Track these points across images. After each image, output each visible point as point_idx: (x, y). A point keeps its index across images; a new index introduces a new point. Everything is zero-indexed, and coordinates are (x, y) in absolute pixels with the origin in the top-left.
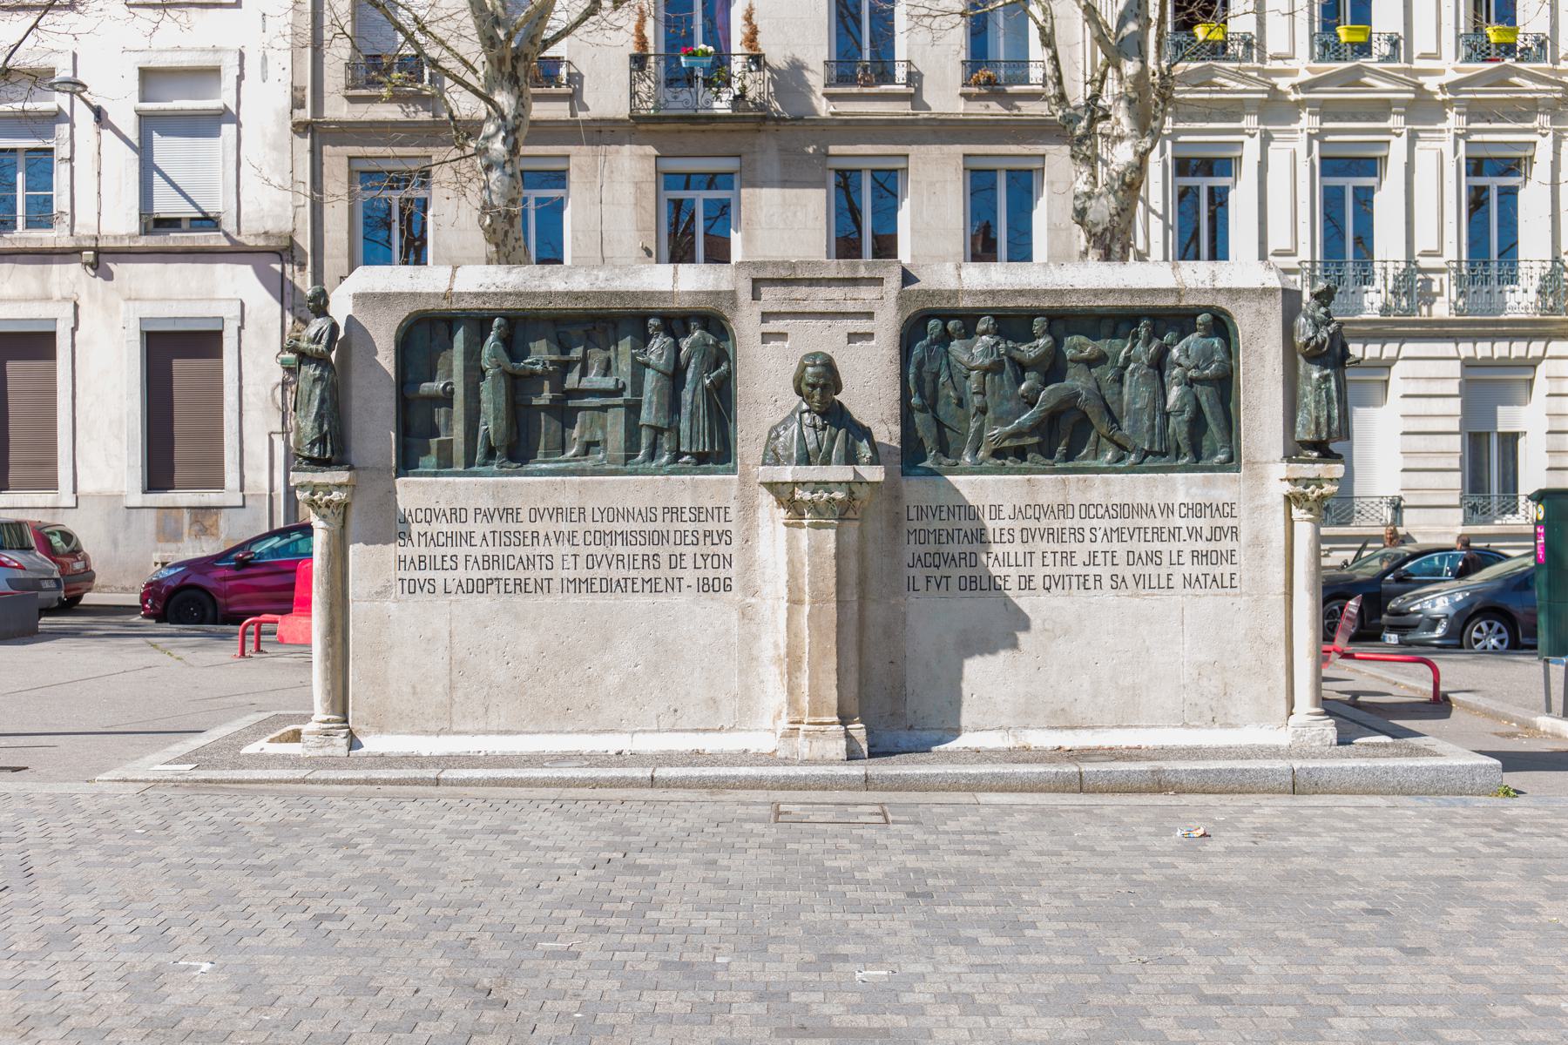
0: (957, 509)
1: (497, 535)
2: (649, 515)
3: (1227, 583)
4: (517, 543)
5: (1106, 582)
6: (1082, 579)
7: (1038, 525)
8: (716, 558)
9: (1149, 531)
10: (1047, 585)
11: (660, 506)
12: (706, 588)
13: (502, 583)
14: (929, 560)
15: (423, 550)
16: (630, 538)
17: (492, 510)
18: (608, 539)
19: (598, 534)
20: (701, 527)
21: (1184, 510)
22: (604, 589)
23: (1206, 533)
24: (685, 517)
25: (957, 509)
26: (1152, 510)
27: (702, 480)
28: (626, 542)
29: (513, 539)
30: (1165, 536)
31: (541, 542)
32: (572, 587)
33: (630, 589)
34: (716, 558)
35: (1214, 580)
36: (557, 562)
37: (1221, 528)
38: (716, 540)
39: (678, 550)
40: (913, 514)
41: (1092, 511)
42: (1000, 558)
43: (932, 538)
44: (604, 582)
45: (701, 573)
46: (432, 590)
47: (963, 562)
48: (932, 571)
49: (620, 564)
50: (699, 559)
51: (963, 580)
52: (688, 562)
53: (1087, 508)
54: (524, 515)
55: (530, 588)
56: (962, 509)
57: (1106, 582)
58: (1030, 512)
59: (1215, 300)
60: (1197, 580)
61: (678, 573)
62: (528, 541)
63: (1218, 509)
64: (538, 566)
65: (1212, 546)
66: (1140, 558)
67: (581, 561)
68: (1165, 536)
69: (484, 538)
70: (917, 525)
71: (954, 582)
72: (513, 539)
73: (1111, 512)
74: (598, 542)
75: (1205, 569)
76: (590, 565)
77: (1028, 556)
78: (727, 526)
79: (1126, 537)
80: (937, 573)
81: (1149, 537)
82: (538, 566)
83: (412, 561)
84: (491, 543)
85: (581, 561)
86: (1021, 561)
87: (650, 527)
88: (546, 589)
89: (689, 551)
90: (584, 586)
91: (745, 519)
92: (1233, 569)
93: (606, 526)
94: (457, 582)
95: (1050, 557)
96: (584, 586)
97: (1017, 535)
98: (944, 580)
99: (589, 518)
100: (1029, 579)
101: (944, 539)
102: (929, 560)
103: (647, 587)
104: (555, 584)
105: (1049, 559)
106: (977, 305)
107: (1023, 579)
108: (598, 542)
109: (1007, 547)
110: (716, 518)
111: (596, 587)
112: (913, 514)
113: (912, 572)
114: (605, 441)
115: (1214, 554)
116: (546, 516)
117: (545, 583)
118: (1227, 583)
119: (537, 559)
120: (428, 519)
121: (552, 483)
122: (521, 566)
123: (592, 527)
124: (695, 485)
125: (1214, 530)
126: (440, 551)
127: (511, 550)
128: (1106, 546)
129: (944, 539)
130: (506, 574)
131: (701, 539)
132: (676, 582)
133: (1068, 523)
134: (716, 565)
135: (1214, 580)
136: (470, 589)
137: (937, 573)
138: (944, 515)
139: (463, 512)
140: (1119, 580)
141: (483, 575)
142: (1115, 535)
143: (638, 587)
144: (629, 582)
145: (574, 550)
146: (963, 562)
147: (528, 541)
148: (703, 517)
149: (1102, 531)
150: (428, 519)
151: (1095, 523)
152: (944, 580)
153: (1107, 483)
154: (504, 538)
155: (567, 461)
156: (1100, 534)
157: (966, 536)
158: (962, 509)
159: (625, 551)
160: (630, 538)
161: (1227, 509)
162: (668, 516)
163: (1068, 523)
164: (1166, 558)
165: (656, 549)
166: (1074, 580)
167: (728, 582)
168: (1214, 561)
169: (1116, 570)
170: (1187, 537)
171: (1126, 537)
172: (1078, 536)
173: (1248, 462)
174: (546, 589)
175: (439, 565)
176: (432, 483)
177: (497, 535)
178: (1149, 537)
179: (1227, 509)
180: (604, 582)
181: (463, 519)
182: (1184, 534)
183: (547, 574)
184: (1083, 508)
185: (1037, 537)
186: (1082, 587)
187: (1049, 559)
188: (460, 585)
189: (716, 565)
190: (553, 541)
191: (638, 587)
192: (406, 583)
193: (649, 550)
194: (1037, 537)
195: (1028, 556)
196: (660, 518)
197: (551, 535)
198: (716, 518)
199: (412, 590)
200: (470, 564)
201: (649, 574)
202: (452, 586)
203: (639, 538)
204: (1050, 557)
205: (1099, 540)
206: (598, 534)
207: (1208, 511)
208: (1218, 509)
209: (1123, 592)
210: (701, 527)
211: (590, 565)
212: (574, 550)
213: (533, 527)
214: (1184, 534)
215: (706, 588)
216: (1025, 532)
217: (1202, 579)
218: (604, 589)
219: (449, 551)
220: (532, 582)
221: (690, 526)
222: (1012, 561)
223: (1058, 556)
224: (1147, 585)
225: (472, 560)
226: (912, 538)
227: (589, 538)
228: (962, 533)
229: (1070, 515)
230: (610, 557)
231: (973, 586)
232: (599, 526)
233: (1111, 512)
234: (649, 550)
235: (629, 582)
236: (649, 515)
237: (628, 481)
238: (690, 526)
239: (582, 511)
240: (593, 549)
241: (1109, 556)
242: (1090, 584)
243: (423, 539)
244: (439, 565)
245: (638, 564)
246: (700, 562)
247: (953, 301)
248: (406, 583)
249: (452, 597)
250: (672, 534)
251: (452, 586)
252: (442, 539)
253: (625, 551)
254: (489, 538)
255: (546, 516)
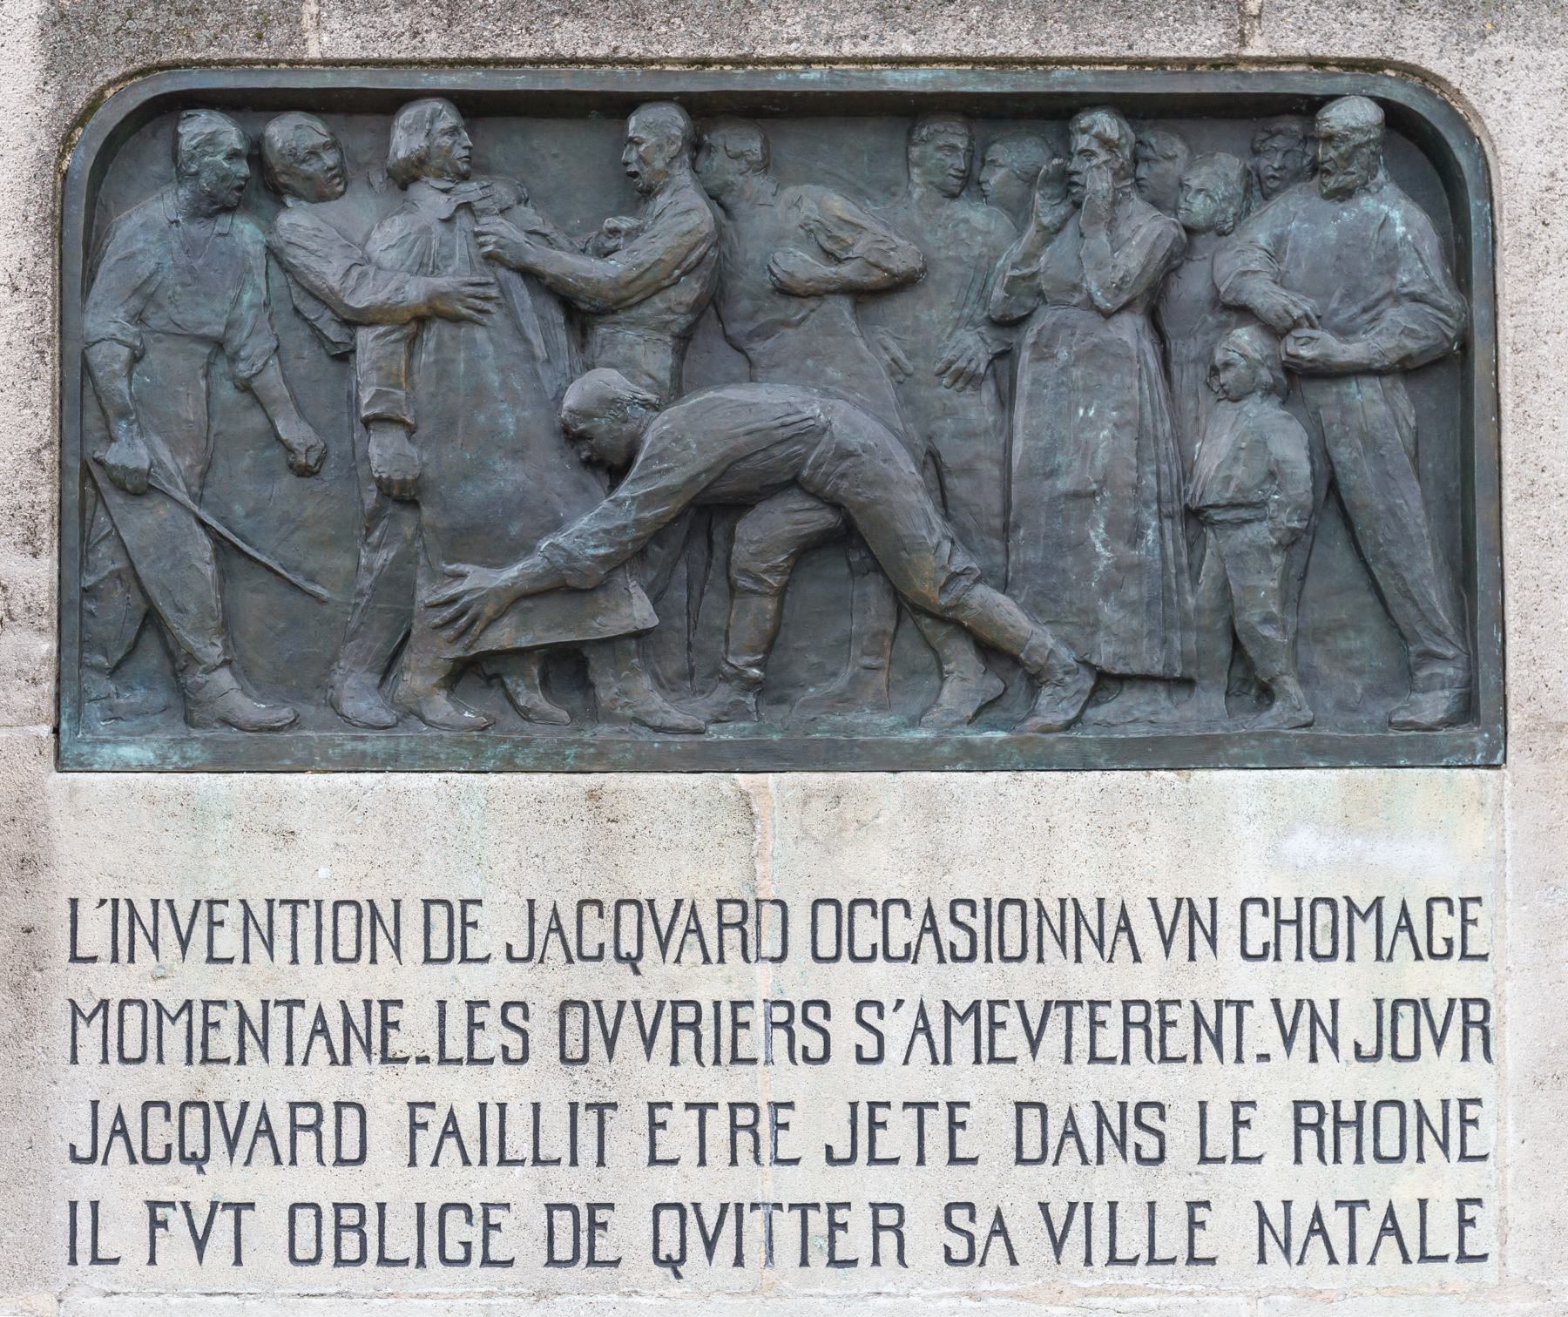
0: (282, 915)
3: (1443, 1239)
5: (926, 1234)
6: (818, 1221)
7: (631, 987)
9: (1112, 1016)
10: (670, 1247)
14: (162, 1132)
21: (1261, 929)
23: (1357, 1027)
25: (282, 915)
26: (1125, 926)
30: (1180, 1040)
35: (1390, 1226)
37: (1420, 1006)
40: (95, 935)
41: (867, 930)
42: (468, 1126)
43: (175, 1036)
47: (306, 1141)
48: (174, 1182)
51: (305, 1218)
53: (846, 914)
56: (307, 917)
57: (926, 1234)
58: (597, 932)
59: (1390, 36)
60: (1317, 1226)
63: (1405, 923)
65: (1382, 1080)
66: (1071, 1130)
68: (1180, 1040)
70: (114, 982)
71: (266, 1229)
73: (948, 932)
75: (1349, 1179)
77: (588, 1122)
79: (1011, 1041)
80: (198, 1189)
81: (1110, 1042)
86: (555, 1142)
92: (1469, 1180)
95: (682, 1124)
97: (542, 1029)
98: (225, 1219)
100: (593, 1218)
101: (224, 1042)
102: (162, 1132)
105: (679, 1135)
106: (382, 50)
107: (563, 1220)
109: (501, 1083)
112: (95, 935)
113: (88, 1182)
115: (1390, 1116)
118: (1443, 1239)
125: (1388, 1012)
128: (923, 1080)
129: (224, 1042)
133: (762, 982)
135: (1390, 1226)
137: (198, 1189)
138: (228, 943)
140: (981, 1229)
142: (963, 1035)
146: (306, 1141)
149: (909, 1015)
151: (879, 979)
152: (225, 1219)
153: (932, 812)
156: (898, 1028)
157: (320, 1028)
158: (307, 917)
161: (1447, 926)
163: (762, 982)
164: (1181, 1133)
166: (787, 1224)
168: (1390, 1147)
169: (961, 1183)
170: (1274, 1043)
171: (1011, 1041)
172: (805, 1036)
173: (1540, 723)
178: (1110, 1042)
179: (1447, 926)
182: (1262, 1031)
184: (827, 914)
185: (629, 1037)
186: (818, 1257)
187: (679, 1135)
194: (629, 1037)
195: (588, 1122)
204: (682, 1124)
205: (894, 1052)
207: (1365, 932)
208: (1405, 923)
209: (994, 1274)
214: (1262, 1031)
216: (575, 1019)
217: (1336, 1222)
222: (519, 1145)
223: (718, 1123)
224: (1100, 1252)
226: (89, 1036)
228: (304, 1020)
229: (771, 947)
231: (350, 1249)
233: (948, 932)
241: (937, 1122)
242: (856, 1241)
247: (279, 33)
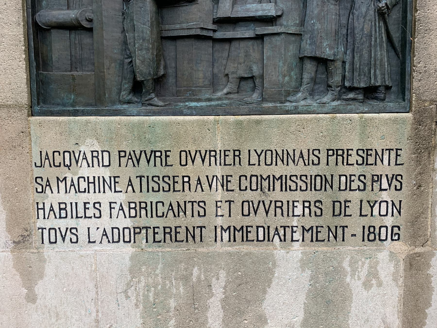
1: (144, 180)
2: (312, 157)
4: (167, 188)
8: (384, 205)
11: (323, 148)
12: (372, 237)
13: (151, 231)
15: (63, 197)
16: (289, 182)
17: (138, 153)
18: (265, 184)
19: (254, 179)
20: (369, 171)
22: (261, 238)
24: (352, 160)
27: (371, 119)
28: (285, 188)
29: (162, 184)
31: (193, 187)
32: (226, 236)
33: (288, 237)
34: (384, 205)
36: (211, 209)
38: (385, 185)
39: (342, 196)
44: (261, 230)
45: (366, 221)
46: (74, 240)
49: (279, 211)
50: (365, 205)
52: (353, 209)
54: (173, 159)
55: (181, 236)
61: (342, 221)
62: (179, 187)
64: (189, 212)
67: (236, 208)
69: (130, 183)
72: (162, 184)
74: (254, 187)
76: (246, 212)
78: (397, 170)
82: (189, 212)
83: (52, 209)
84: (137, 188)
85: (236, 208)
87: (313, 171)
88: (198, 238)
89: (355, 196)
90: (238, 235)
91: (418, 162)
93: (264, 171)
94: (101, 231)
96: (238, 235)
99: (245, 161)
103: (308, 235)
104: (208, 234)
108: (254, 187)
110: (386, 161)
111: (252, 236)
114: (262, 77)
116: (198, 159)
117: (197, 231)
119: (189, 206)
120: (67, 162)
121: (205, 123)
122: (171, 213)
123: (249, 171)
124: (364, 124)
126: (82, 198)
127: (160, 197)
130: (154, 222)
131: (369, 183)
132: (340, 231)
134: (383, 212)
136: (116, 239)
139: (106, 155)
141: (129, 223)
143: (297, 236)
144: (288, 231)
145: (229, 196)
147: (179, 187)
148: (371, 160)
150: (67, 162)
154: (152, 184)
155: (219, 99)
159: (284, 197)
160: (289, 182)
162: (332, 159)
165: (318, 196)
167: (396, 230)
174: (198, 238)
175: (81, 213)
176: (69, 122)
177: (144, 180)
180: (261, 230)
181: (106, 163)
183: (199, 222)
188: (105, 234)
189: (383, 212)
190: (206, 186)
191: (297, 236)
192: (46, 233)
193: (312, 196)
196: (323, 160)
197: (204, 180)
198: (386, 161)
199: (53, 240)
200: (115, 212)
201: (310, 222)
202: (96, 235)
203: (300, 183)
206: (254, 179)
210: (369, 171)
211: (246, 212)
212: (229, 196)
213: (182, 171)
215: (372, 237)
218: (261, 238)
219: (92, 197)
220: (182, 231)
221: (356, 170)
225: (117, 207)
227: (245, 183)
230: (267, 203)
232: (256, 170)
234: (312, 196)
235: (288, 231)
236: (312, 157)
237: (288, 120)
238: (356, 170)
239: (237, 153)
240: (249, 195)
243: (62, 185)
244: (81, 213)
245: (298, 211)
246: (366, 210)
248: (46, 233)
249: (96, 247)
250: (336, 178)
251: (96, 235)
252: (83, 185)
253: (284, 197)
254: (136, 183)
255: (198, 159)
